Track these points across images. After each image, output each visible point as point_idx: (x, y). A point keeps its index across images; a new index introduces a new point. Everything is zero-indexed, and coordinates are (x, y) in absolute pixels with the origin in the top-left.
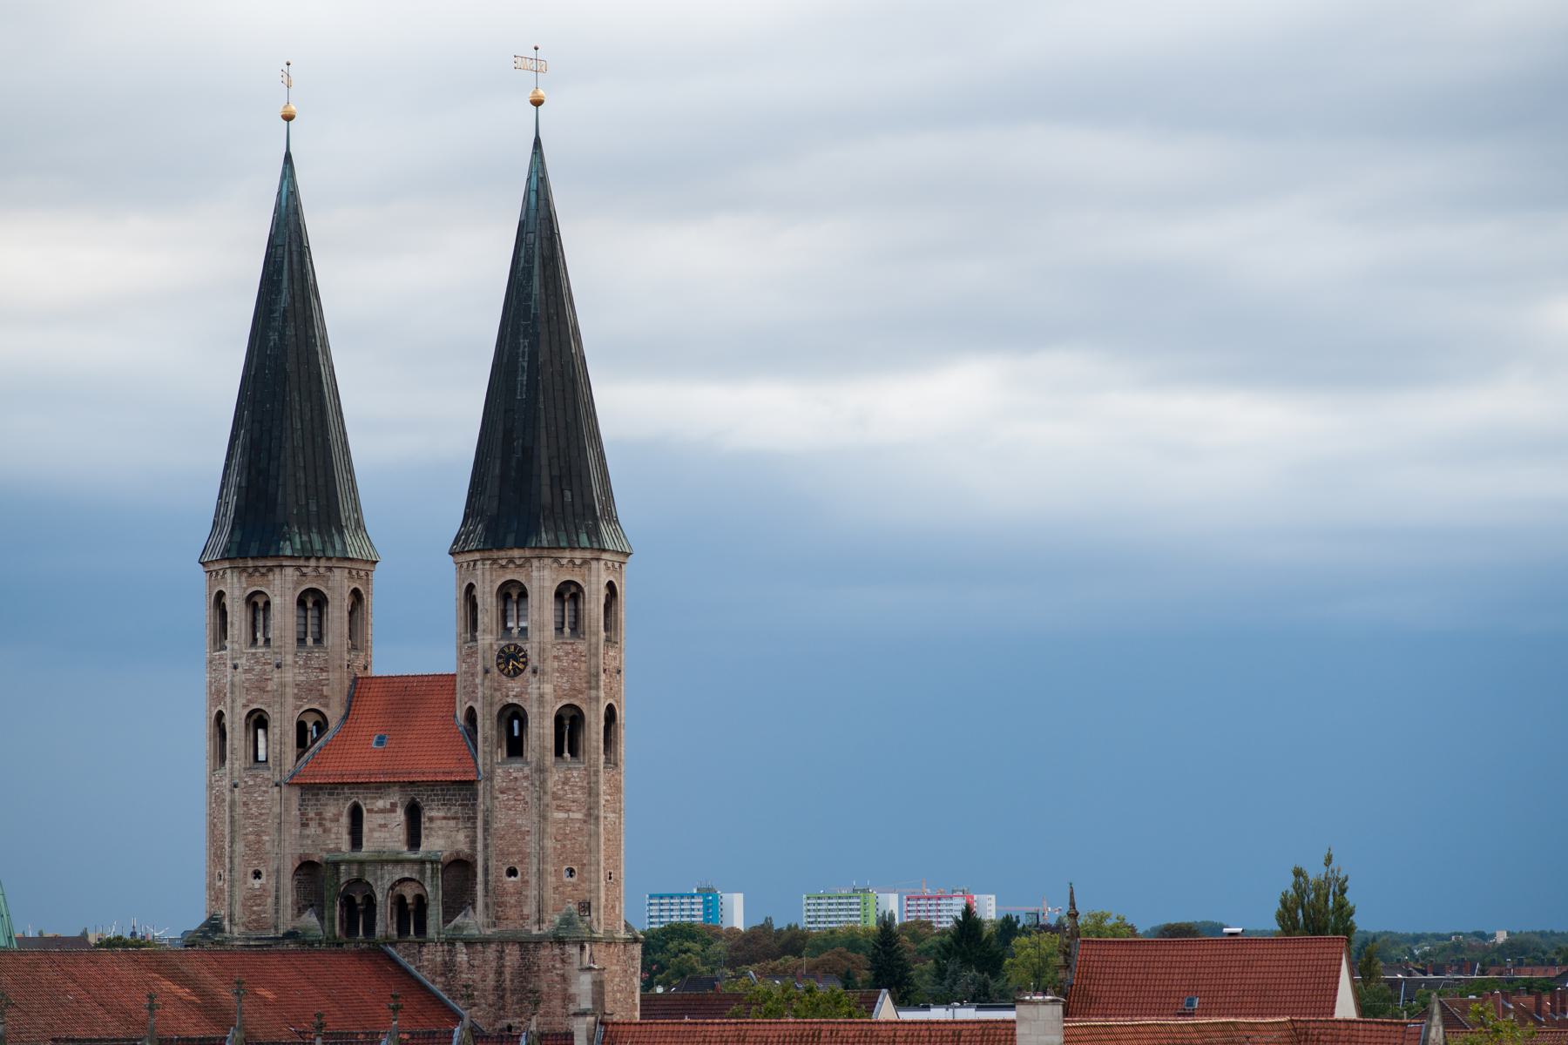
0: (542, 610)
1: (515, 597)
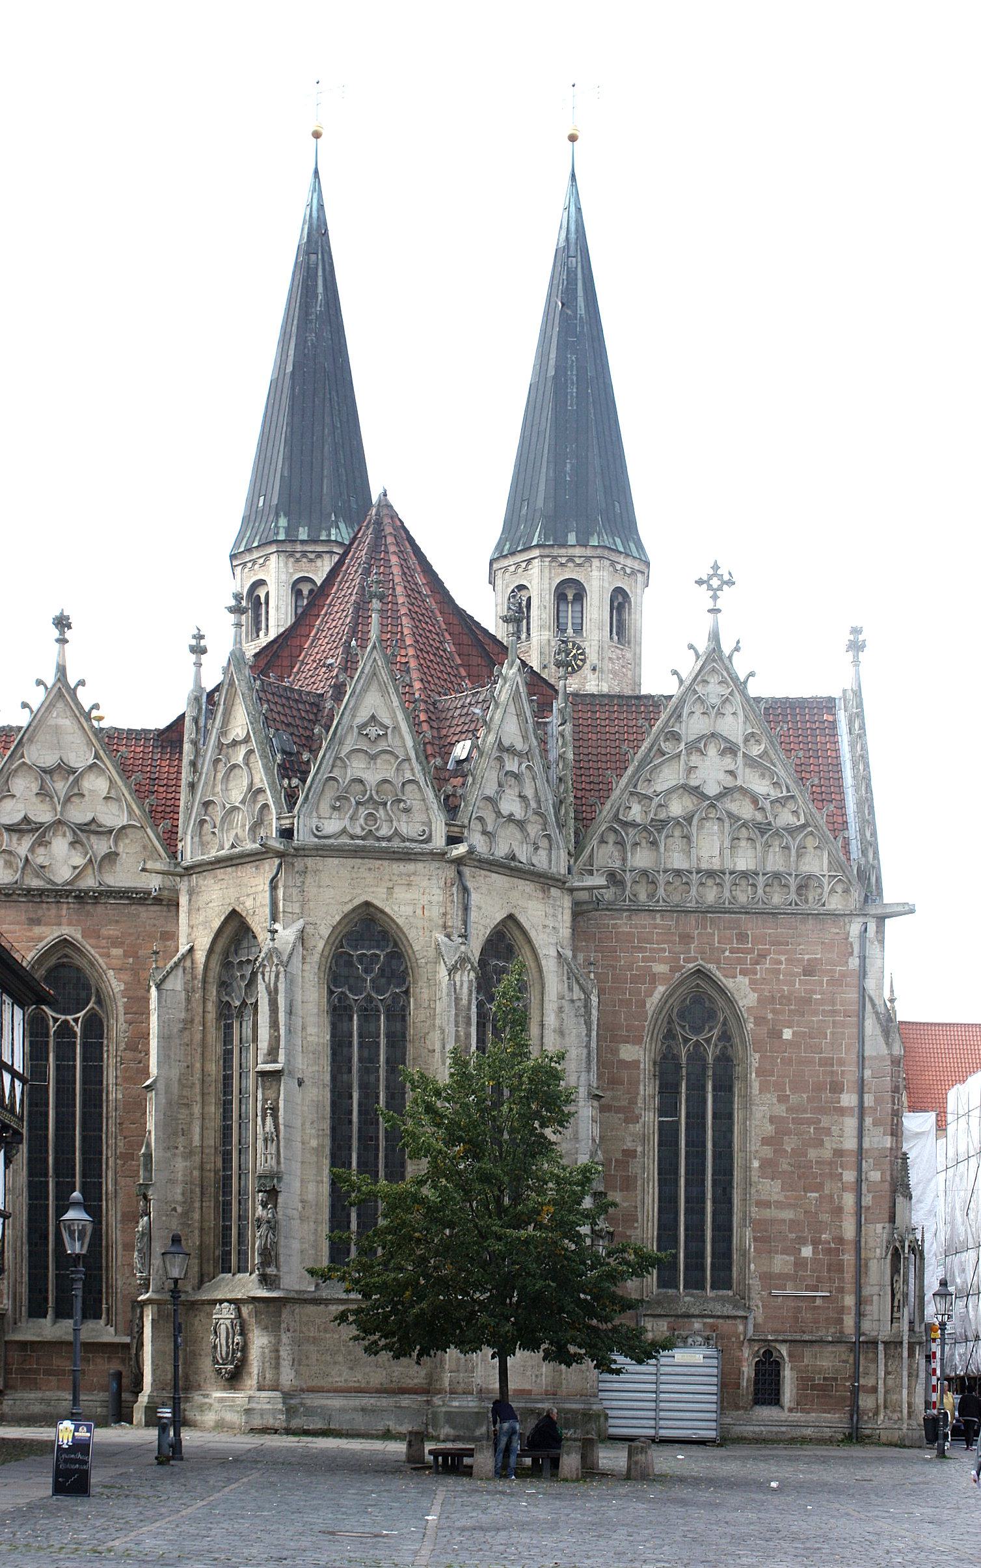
0: (596, 610)
1: (570, 597)
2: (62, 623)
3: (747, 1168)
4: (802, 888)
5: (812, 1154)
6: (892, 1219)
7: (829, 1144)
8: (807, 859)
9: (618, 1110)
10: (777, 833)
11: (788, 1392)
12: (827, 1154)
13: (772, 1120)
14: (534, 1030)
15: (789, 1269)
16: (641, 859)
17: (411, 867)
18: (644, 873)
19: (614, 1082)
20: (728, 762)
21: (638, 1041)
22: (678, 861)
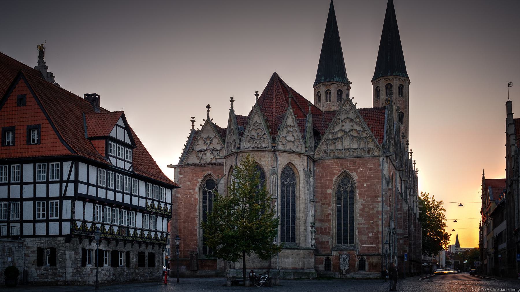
0: (395, 90)
2: (208, 107)
3: (357, 216)
4: (369, 151)
5: (371, 212)
6: (389, 227)
7: (375, 210)
8: (370, 144)
9: (327, 204)
10: (362, 139)
11: (367, 267)
12: (375, 212)
13: (362, 204)
14: (298, 187)
15: (367, 239)
16: (332, 147)
17: (264, 153)
18: (332, 150)
19: (326, 198)
20: (351, 124)
21: (331, 188)
22: (340, 147)
